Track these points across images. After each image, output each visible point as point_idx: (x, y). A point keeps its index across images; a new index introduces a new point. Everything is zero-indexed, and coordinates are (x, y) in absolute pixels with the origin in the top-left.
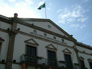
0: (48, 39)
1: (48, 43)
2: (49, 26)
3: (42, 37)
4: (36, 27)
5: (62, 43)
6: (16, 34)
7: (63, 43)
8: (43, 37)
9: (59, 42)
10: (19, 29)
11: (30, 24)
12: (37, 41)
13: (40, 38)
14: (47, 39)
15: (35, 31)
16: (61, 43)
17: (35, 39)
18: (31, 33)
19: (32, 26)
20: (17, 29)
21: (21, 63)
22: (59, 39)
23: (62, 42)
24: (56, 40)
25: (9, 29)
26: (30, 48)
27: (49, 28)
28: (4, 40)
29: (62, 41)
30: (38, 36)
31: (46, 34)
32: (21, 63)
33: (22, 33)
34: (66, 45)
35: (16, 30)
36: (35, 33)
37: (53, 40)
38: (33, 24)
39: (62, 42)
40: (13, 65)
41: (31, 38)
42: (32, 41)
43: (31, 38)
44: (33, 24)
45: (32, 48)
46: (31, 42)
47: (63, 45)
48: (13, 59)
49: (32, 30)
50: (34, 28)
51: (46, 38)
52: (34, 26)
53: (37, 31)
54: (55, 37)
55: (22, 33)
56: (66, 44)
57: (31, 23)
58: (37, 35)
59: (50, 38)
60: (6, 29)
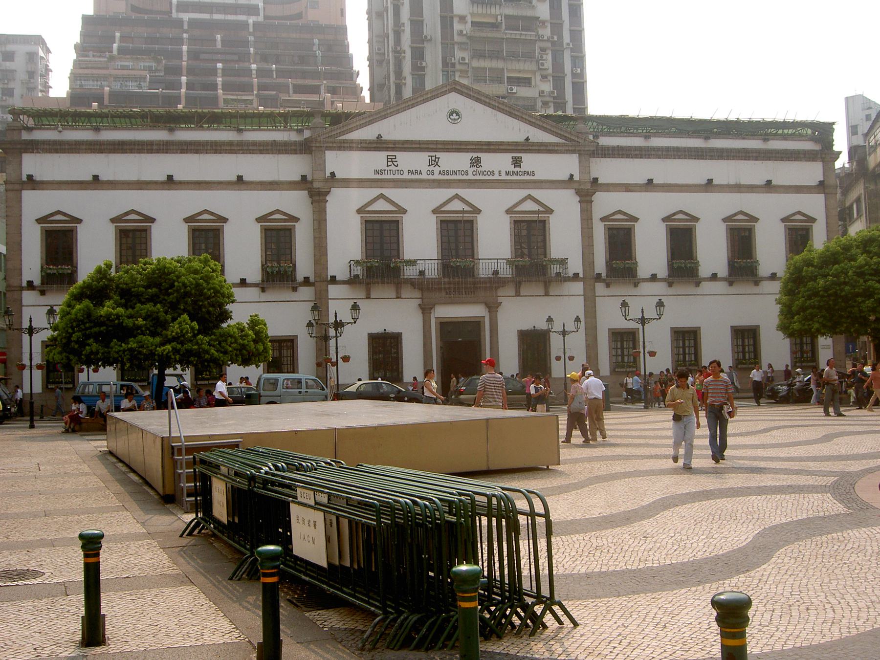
0: (446, 177)
1: (441, 195)
2: (451, 114)
3: (420, 177)
4: (395, 142)
5: (509, 178)
6: (328, 193)
7: (515, 173)
8: (424, 176)
9: (496, 177)
10: (333, 174)
11: (371, 142)
12: (398, 195)
13: (412, 181)
14: (441, 177)
15: (391, 160)
16: (504, 177)
17: (389, 192)
18: (376, 172)
19: (378, 145)
20: (328, 174)
21: (353, 281)
22: (497, 164)
23: (507, 173)
24: (483, 173)
25: (304, 177)
26: (377, 226)
27: (454, 122)
28: (296, 219)
29: (512, 168)
30: (406, 176)
31: (438, 155)
32: (353, 281)
33: (346, 183)
34: (532, 178)
35: (326, 180)
36: (393, 168)
37: (465, 177)
38: (379, 136)
39: (507, 173)
40: (331, 288)
41: (376, 192)
42: (381, 201)
43: (376, 192)
44: (379, 136)
45: (386, 227)
46: (382, 205)
47: (511, 181)
48: (331, 273)
49: (379, 159)
50: (387, 149)
51: (436, 176)
52: (386, 142)
53: (401, 156)
54: (479, 155)
55: (346, 183)
56: (533, 174)
57: (367, 133)
58: (401, 172)
59: (451, 169)
60: (298, 178)
